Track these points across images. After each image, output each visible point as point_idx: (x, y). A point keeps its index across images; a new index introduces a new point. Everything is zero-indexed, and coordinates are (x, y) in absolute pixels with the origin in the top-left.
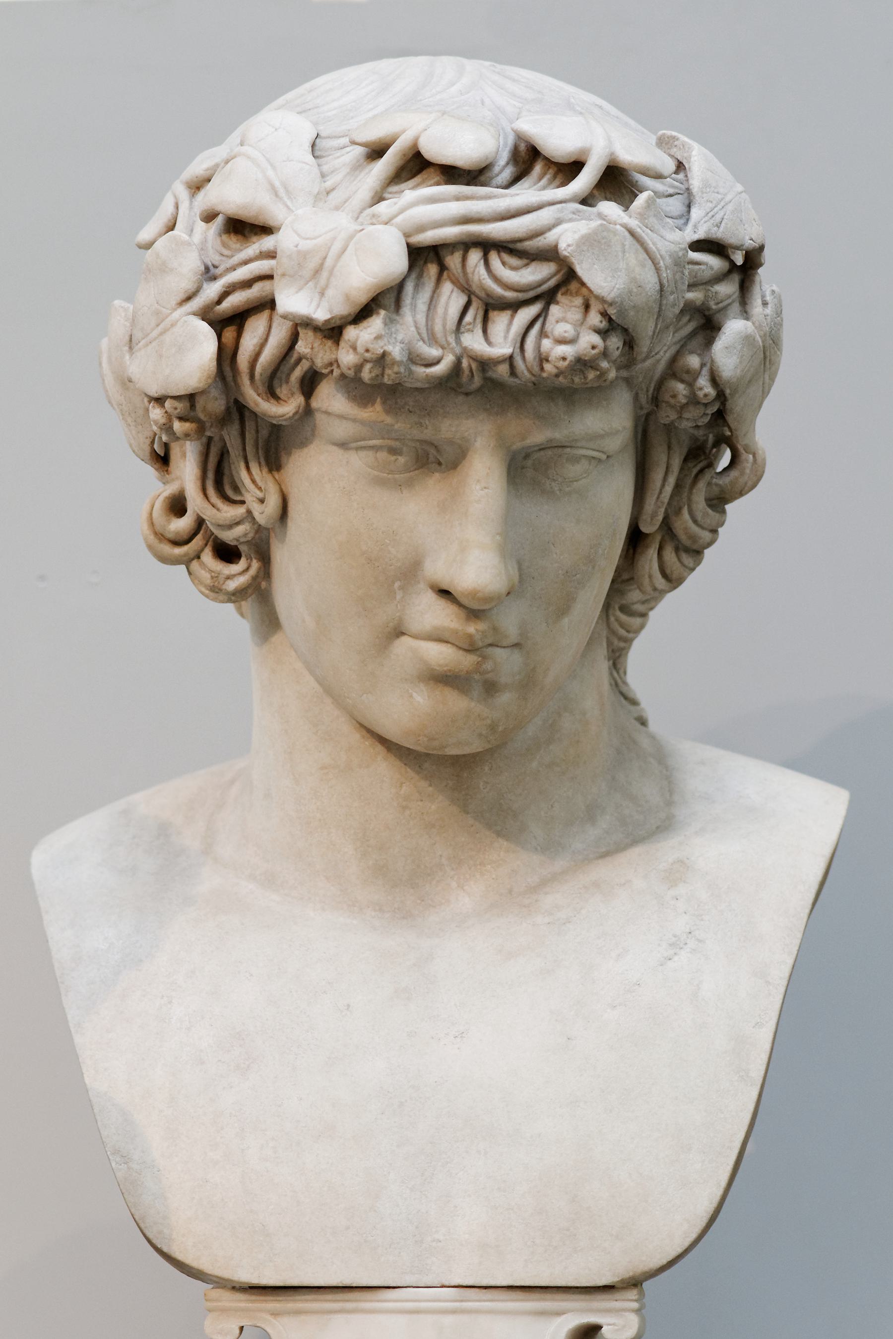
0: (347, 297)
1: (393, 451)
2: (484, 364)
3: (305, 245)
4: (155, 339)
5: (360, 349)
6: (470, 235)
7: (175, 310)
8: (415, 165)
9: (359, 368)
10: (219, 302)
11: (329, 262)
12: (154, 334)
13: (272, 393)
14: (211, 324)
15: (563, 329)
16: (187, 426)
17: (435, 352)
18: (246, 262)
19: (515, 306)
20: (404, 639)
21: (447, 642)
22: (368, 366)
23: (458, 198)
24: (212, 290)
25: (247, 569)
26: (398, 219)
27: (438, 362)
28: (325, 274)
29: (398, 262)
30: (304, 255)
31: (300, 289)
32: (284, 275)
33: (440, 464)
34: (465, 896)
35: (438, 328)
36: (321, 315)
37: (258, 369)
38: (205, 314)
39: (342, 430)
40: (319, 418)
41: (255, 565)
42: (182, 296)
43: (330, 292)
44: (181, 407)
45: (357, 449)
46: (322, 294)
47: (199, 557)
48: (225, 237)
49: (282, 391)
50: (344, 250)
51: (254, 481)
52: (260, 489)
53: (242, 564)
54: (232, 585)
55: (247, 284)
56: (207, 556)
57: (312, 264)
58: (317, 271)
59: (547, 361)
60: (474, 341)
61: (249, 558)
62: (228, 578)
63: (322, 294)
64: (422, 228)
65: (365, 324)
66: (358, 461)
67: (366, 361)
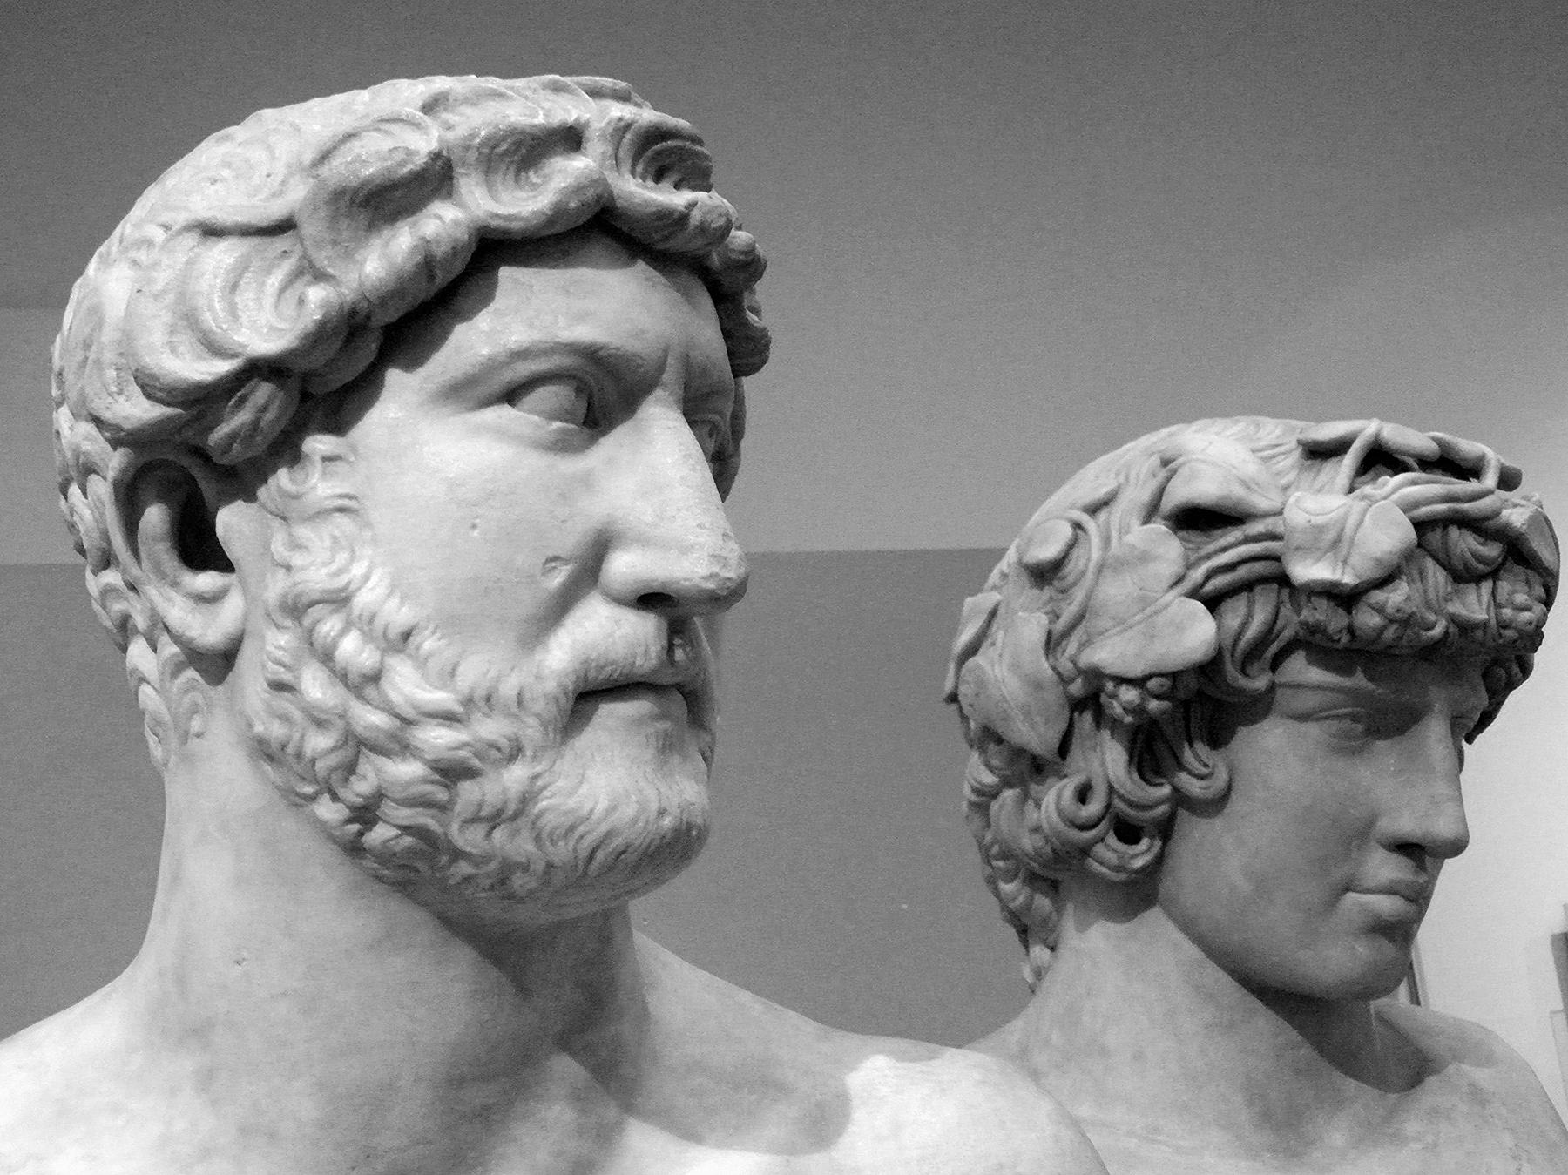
0: (1378, 561)
1: (1355, 718)
2: (1465, 627)
3: (1319, 520)
4: (1139, 623)
5: (1390, 610)
6: (1456, 511)
7: (1166, 592)
8: (1380, 459)
9: (1383, 629)
10: (1202, 585)
11: (1348, 531)
12: (1138, 617)
13: (1244, 672)
14: (1205, 603)
15: (1521, 598)
16: (1165, 704)
17: (1433, 618)
18: (1224, 549)
19: (1478, 579)
20: (1351, 896)
21: (1395, 893)
22: (1395, 626)
23: (1427, 482)
24: (1198, 574)
25: (1148, 850)
26: (1395, 496)
27: (1431, 627)
28: (1344, 546)
29: (1410, 534)
30: (1320, 530)
31: (1319, 559)
32: (1298, 548)
33: (1378, 731)
34: (1337, 1137)
35: (1432, 595)
36: (1349, 579)
37: (1242, 644)
38: (1194, 594)
39: (1309, 701)
40: (1279, 691)
41: (1158, 843)
42: (1174, 579)
43: (1355, 560)
44: (1167, 682)
45: (1318, 720)
46: (1345, 562)
47: (1102, 840)
48: (1183, 534)
49: (1253, 669)
50: (1361, 521)
51: (1200, 761)
52: (1206, 765)
53: (1145, 843)
54: (1138, 863)
55: (1230, 567)
56: (1112, 840)
57: (1330, 536)
58: (1337, 542)
59: (1505, 627)
60: (1455, 608)
61: (1152, 837)
62: (1134, 857)
63: (1345, 562)
64: (1417, 504)
65: (1391, 587)
66: (1313, 729)
67: (1391, 621)
